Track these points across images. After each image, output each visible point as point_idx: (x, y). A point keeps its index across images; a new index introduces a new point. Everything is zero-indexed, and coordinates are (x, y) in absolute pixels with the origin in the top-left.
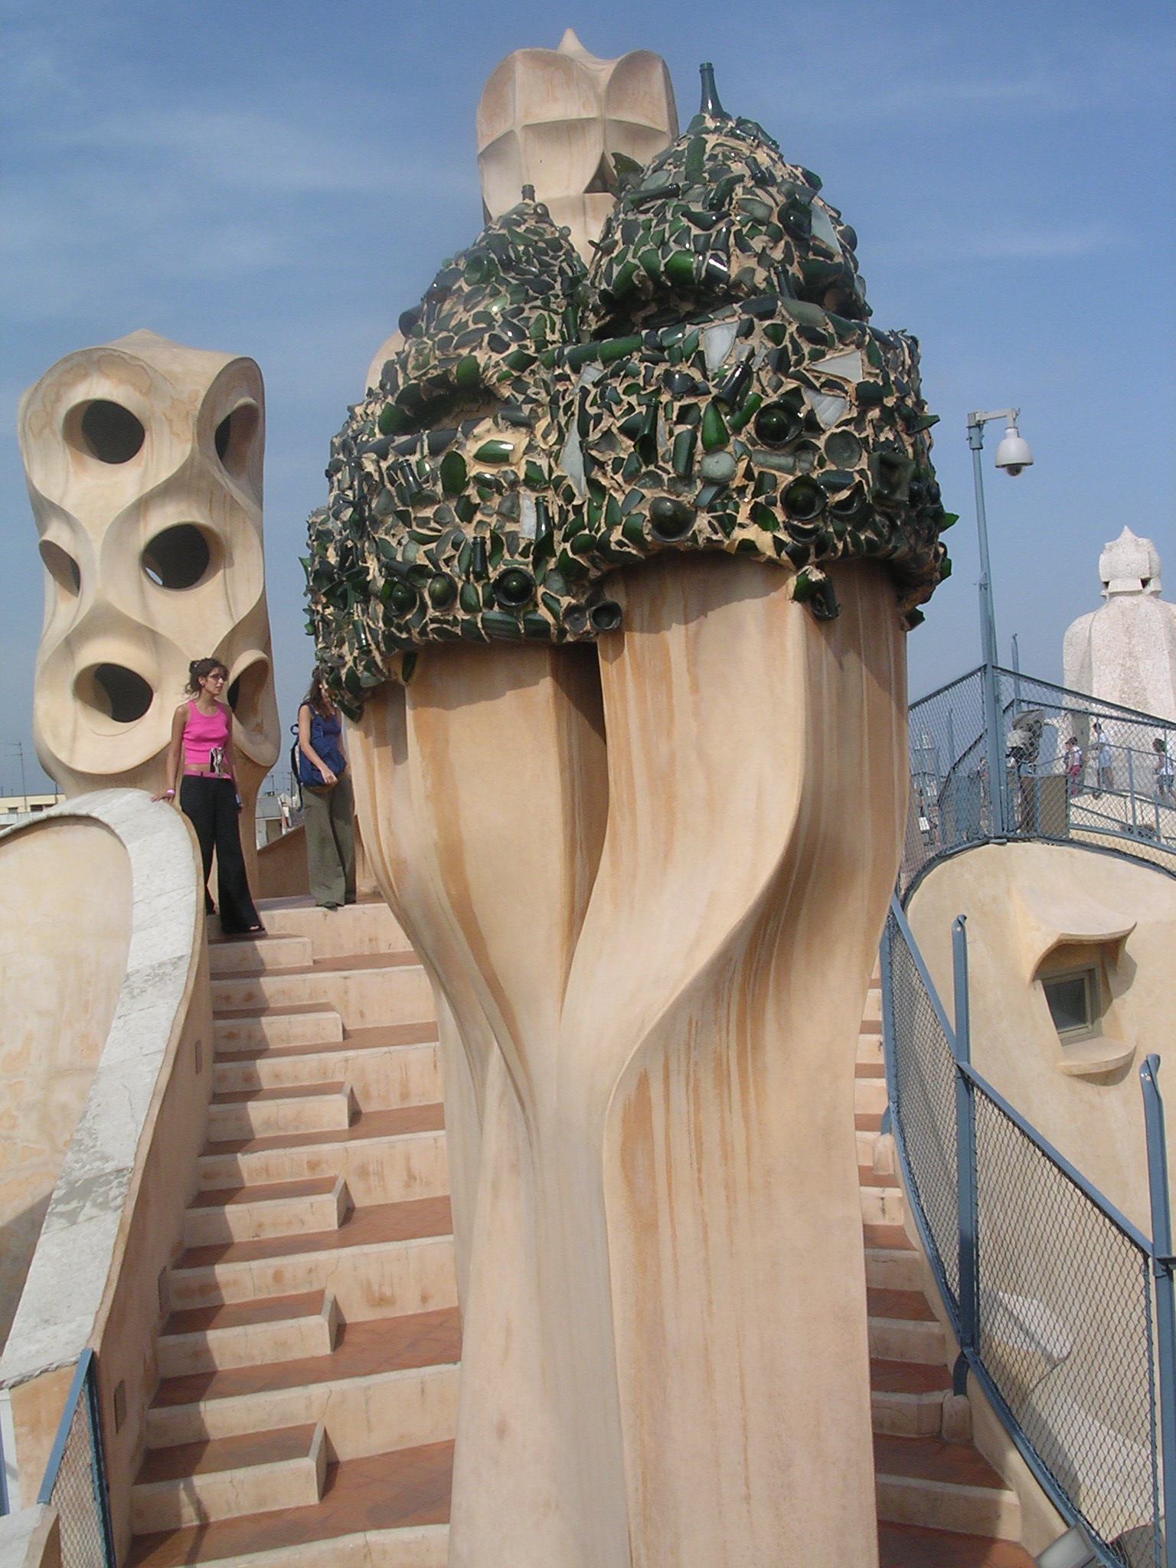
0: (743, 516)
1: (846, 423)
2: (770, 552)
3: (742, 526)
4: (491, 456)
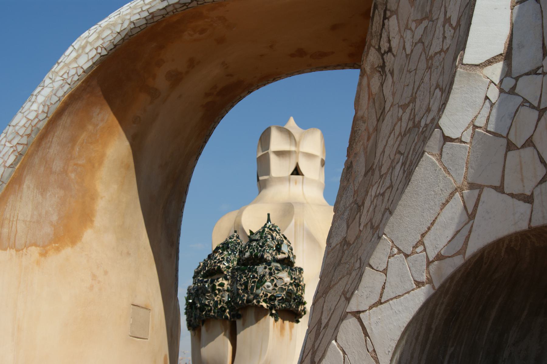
4: (222, 285)
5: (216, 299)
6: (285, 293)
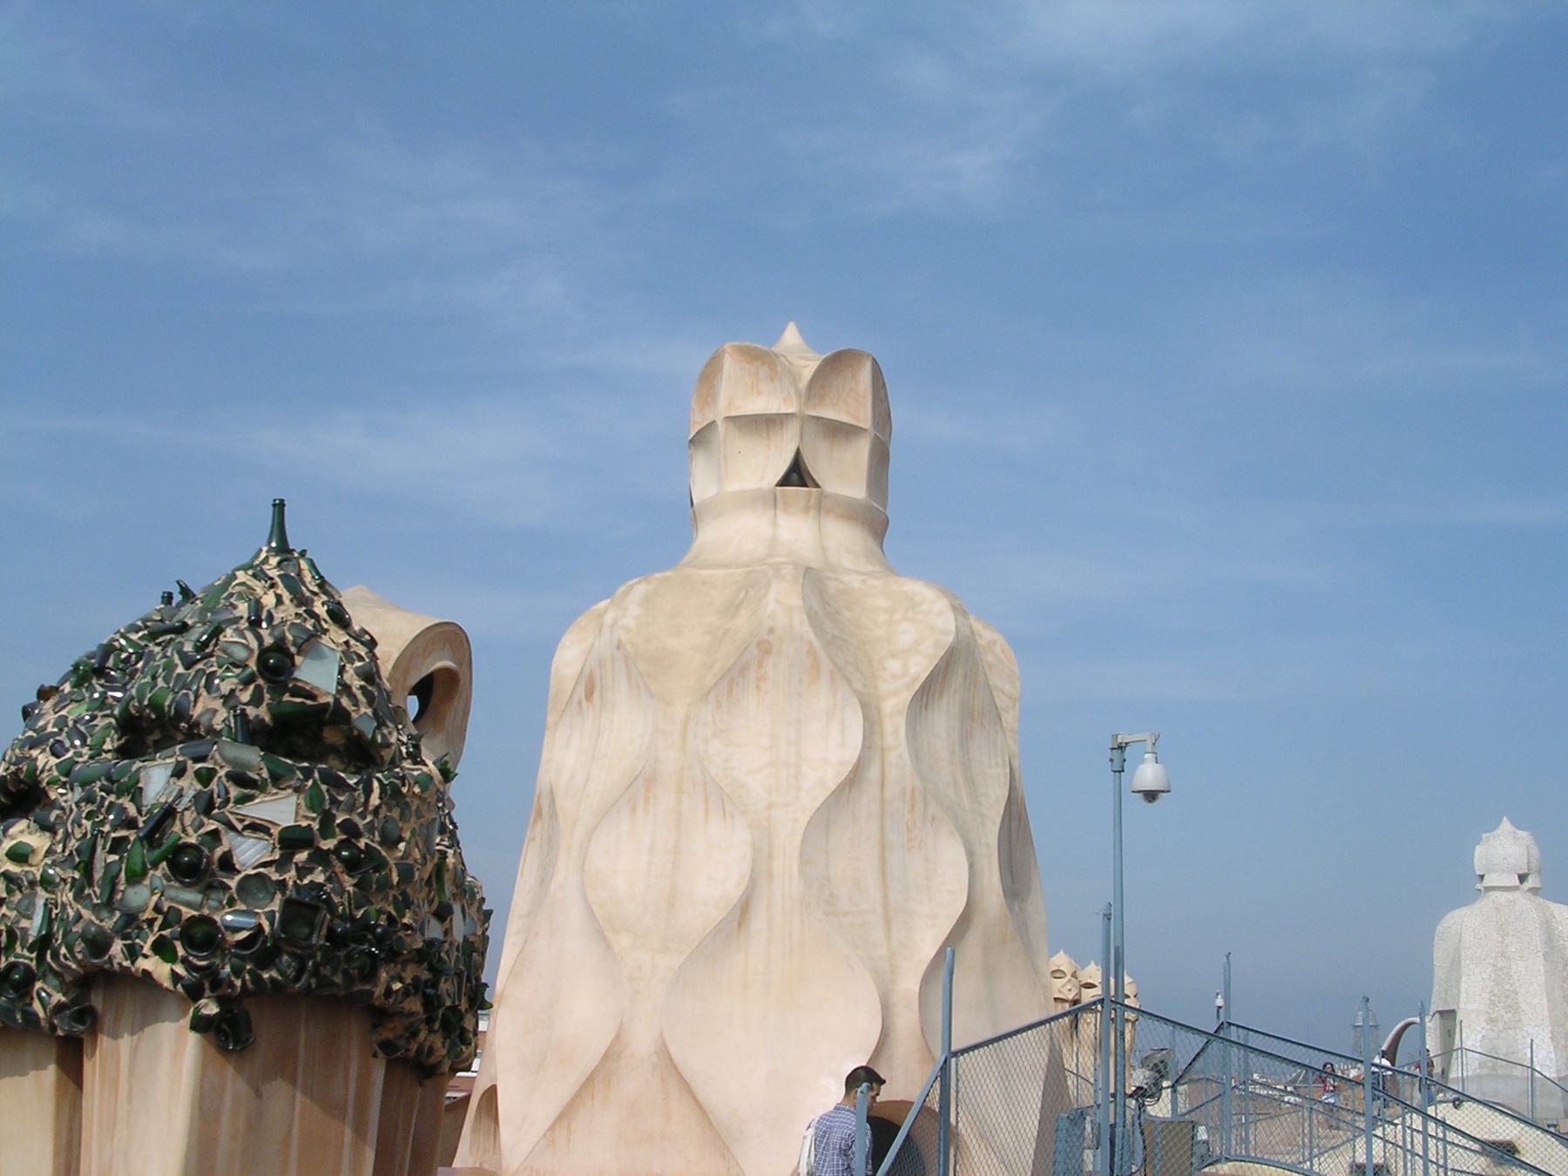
1: (265, 865)
2: (167, 984)
3: (146, 956)
6: (276, 906)
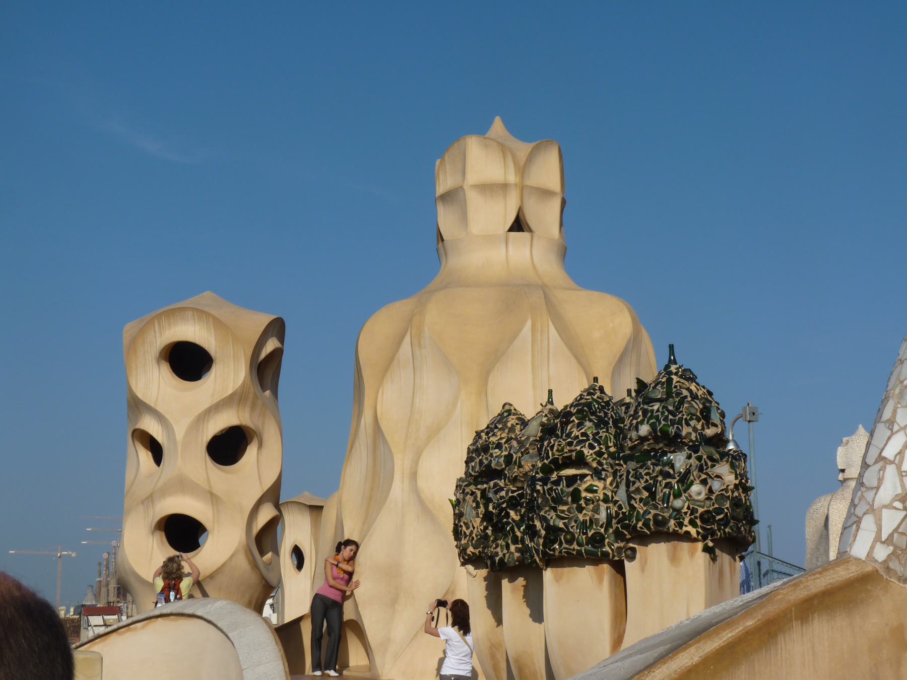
0: (686, 522)
5: (581, 517)
